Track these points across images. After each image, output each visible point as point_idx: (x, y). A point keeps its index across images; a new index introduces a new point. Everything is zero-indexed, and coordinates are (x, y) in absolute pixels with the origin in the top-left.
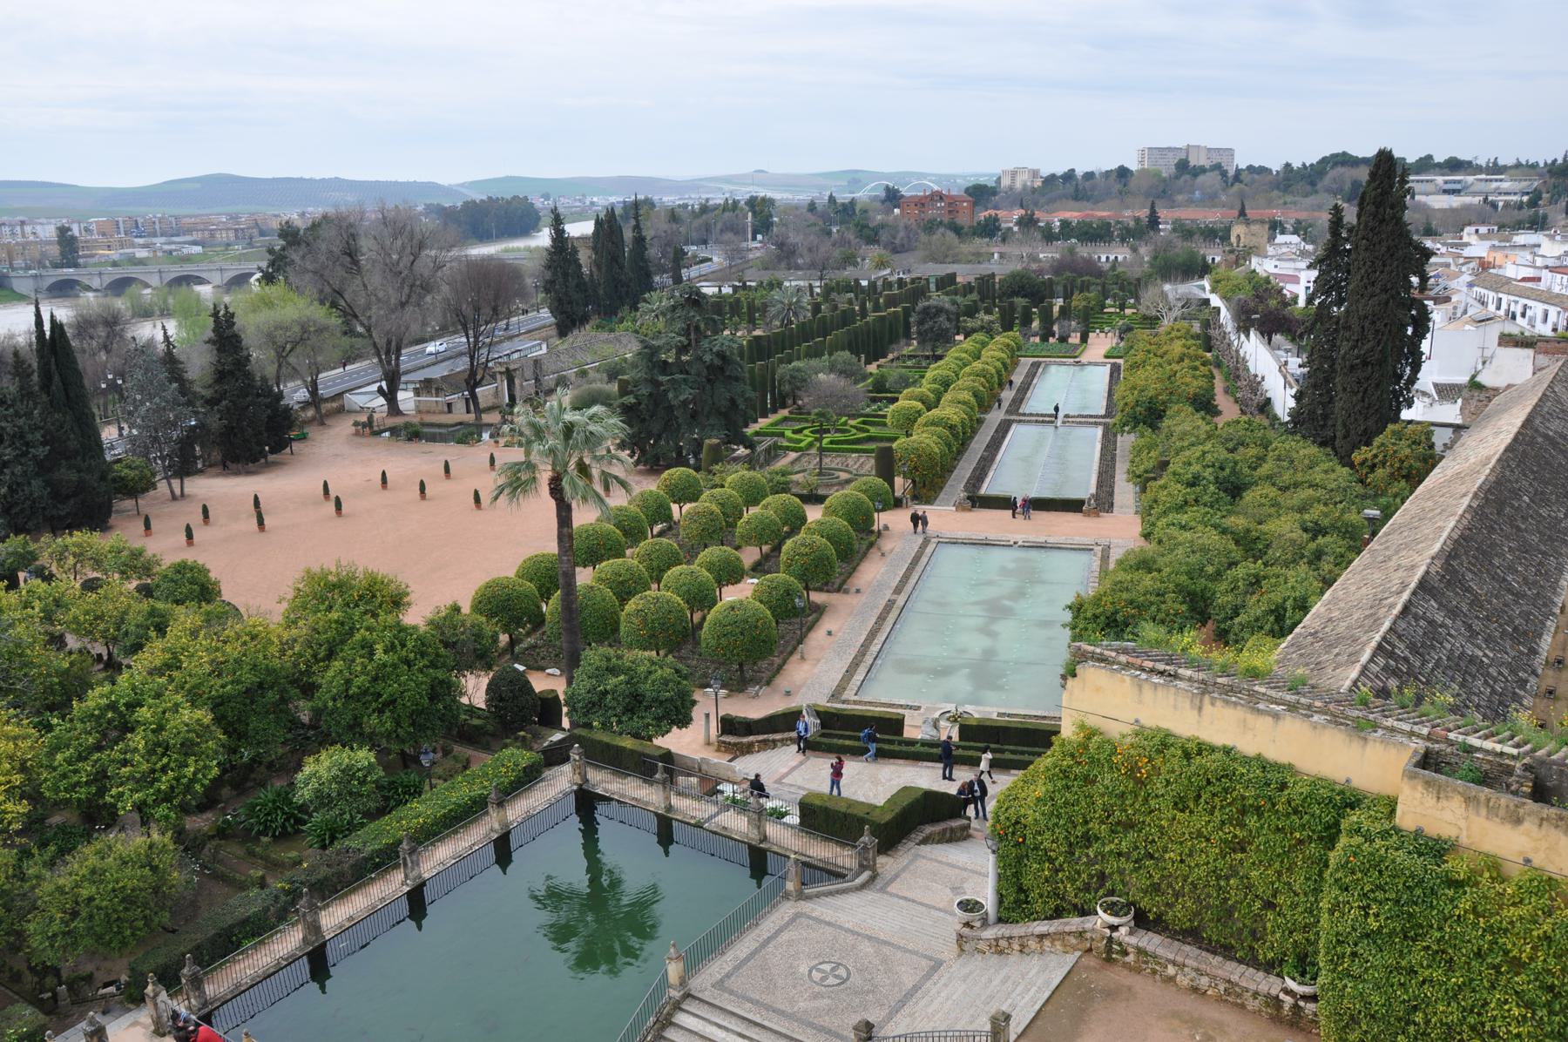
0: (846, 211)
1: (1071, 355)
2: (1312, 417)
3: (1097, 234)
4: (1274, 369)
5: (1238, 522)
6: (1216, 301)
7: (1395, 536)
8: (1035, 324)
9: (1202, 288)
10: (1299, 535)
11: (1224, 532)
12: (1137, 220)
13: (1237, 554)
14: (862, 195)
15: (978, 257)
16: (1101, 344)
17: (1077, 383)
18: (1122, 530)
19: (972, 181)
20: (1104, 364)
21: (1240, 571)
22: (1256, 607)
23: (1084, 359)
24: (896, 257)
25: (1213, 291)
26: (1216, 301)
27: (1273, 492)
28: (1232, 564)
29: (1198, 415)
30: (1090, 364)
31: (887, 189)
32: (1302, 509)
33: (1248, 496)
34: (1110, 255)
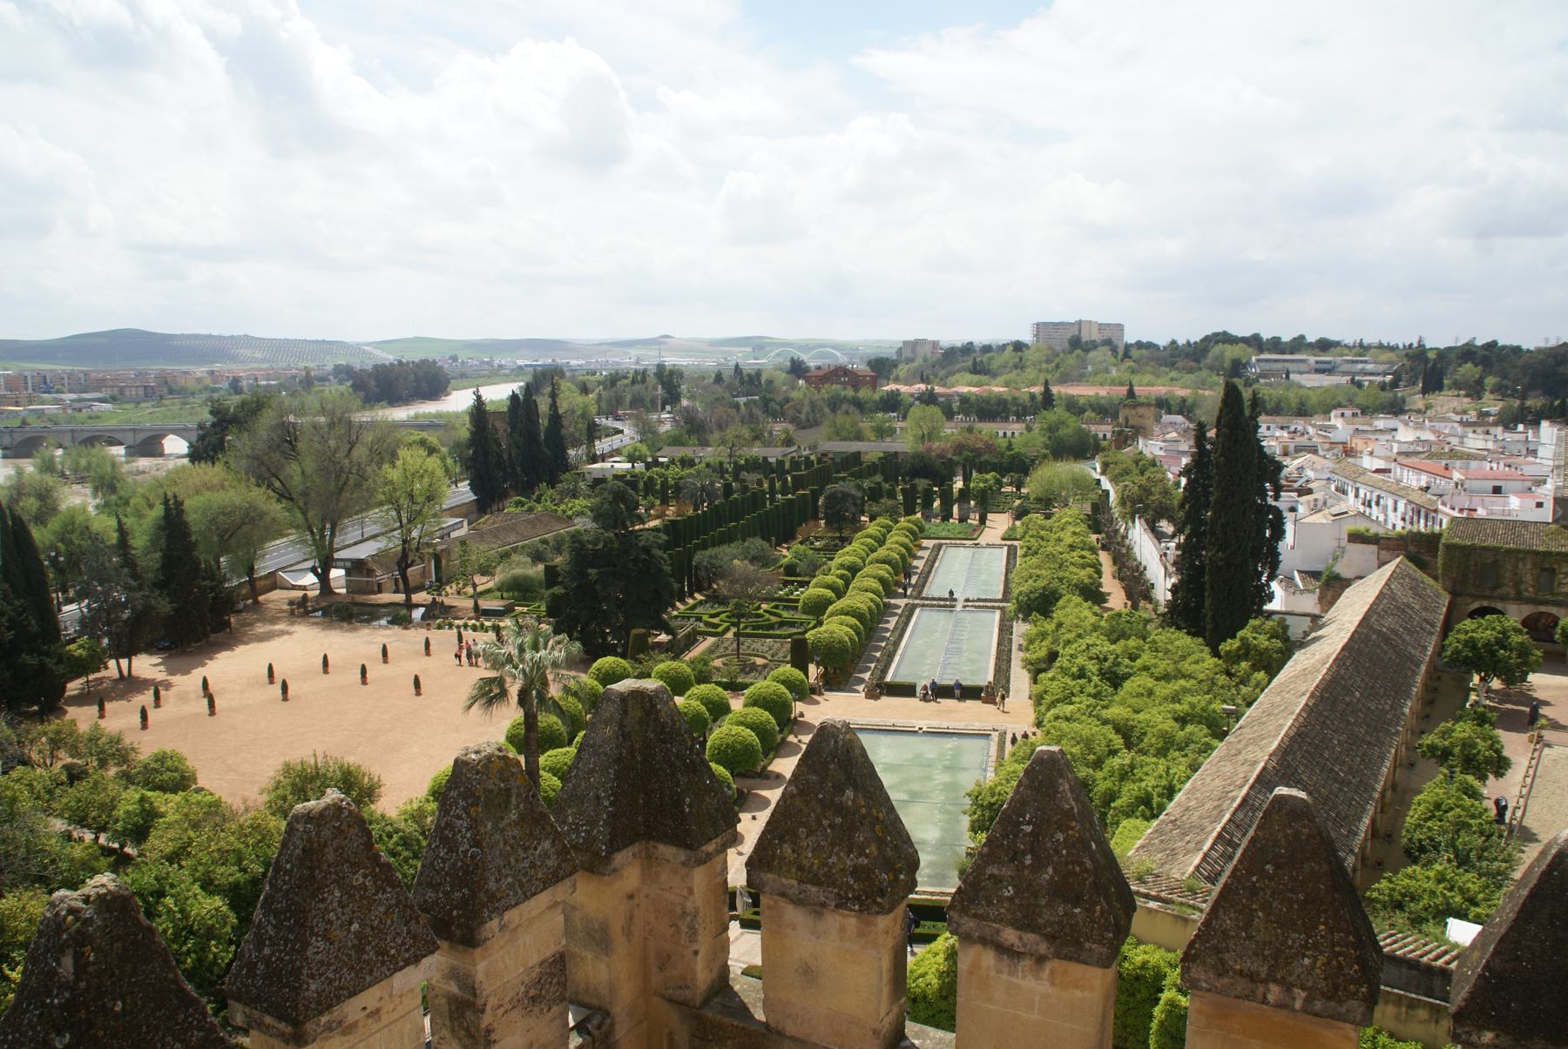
0: (748, 381)
1: (970, 536)
2: (1187, 612)
3: (992, 410)
4: (1154, 554)
5: (1116, 712)
6: (1106, 484)
7: (1246, 730)
8: (937, 504)
9: (1093, 469)
10: (1170, 725)
11: (1105, 722)
12: (1033, 397)
13: (1118, 741)
14: (766, 362)
15: (882, 432)
16: (999, 523)
17: (973, 566)
18: (1018, 713)
19: (874, 352)
20: (1001, 546)
21: (1116, 762)
22: (1128, 792)
23: (982, 540)
24: (803, 433)
25: (1103, 473)
26: (1106, 484)
27: (1150, 683)
28: (1113, 753)
29: (1086, 605)
30: (988, 546)
31: (792, 361)
32: (1175, 698)
33: (1127, 685)
34: (1010, 433)
